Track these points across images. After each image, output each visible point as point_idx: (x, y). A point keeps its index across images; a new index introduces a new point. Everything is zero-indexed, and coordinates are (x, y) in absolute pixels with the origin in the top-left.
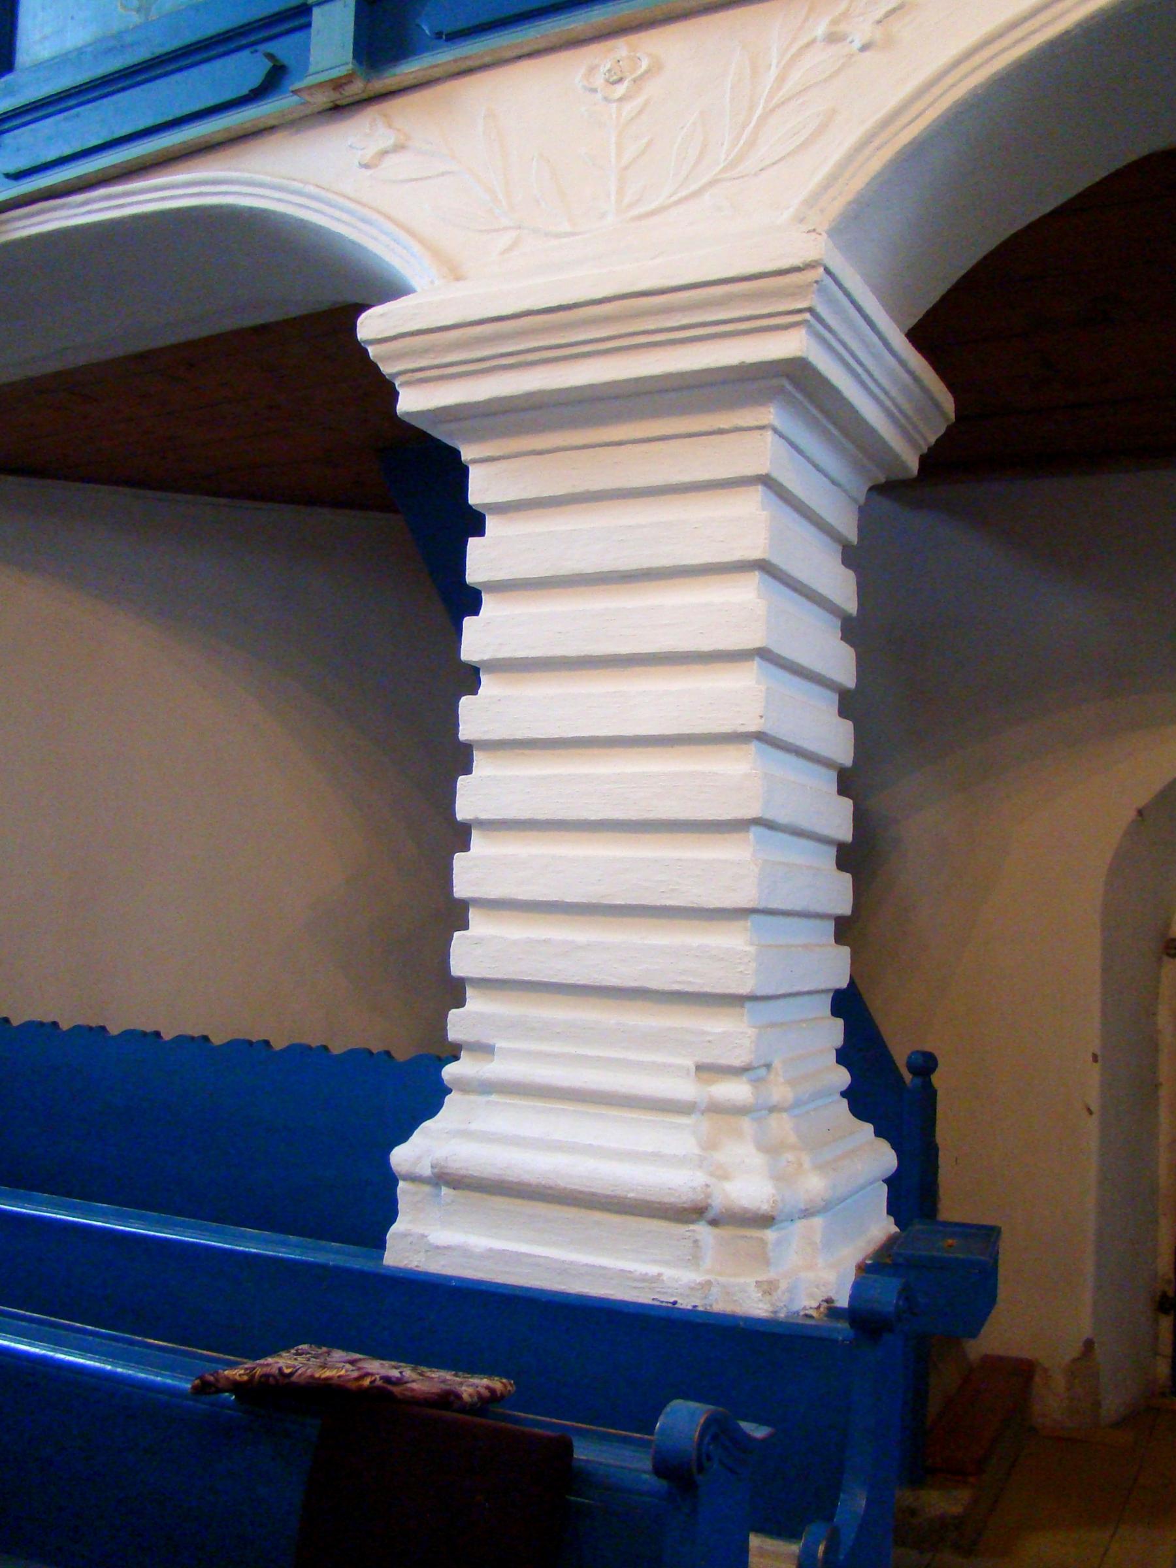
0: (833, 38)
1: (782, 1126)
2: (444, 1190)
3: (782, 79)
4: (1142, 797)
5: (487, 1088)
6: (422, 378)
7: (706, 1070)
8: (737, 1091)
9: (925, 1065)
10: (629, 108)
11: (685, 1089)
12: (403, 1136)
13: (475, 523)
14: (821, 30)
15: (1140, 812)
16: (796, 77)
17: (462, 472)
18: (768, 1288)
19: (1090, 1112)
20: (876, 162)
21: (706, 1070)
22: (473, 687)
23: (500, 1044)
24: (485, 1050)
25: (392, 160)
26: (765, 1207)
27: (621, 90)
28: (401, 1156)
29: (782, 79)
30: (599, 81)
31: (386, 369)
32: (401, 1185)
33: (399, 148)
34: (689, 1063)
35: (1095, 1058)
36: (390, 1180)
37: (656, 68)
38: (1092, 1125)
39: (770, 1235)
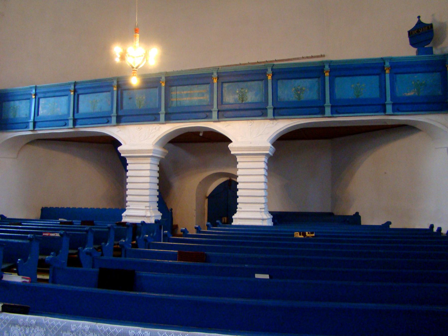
0: (155, 129)
1: (151, 211)
2: (127, 217)
3: (151, 131)
4: (200, 180)
5: (129, 209)
6: (123, 153)
7: (146, 207)
8: (148, 208)
9: (172, 210)
10: (140, 131)
11: (144, 208)
12: (123, 213)
13: (127, 164)
14: (154, 128)
15: (200, 182)
16: (152, 131)
17: (126, 160)
18: (150, 221)
19: (194, 216)
20: (159, 139)
21: (146, 207)
22: (128, 178)
23: (130, 205)
24: (129, 206)
25: (119, 132)
26: (150, 216)
27: (139, 130)
28: (123, 215)
29: (151, 131)
30: (137, 129)
31: (120, 152)
32: (123, 217)
33: (120, 131)
34: (144, 206)
35: (195, 210)
36: (122, 216)
37: (142, 128)
38: (195, 218)
39: (150, 218)
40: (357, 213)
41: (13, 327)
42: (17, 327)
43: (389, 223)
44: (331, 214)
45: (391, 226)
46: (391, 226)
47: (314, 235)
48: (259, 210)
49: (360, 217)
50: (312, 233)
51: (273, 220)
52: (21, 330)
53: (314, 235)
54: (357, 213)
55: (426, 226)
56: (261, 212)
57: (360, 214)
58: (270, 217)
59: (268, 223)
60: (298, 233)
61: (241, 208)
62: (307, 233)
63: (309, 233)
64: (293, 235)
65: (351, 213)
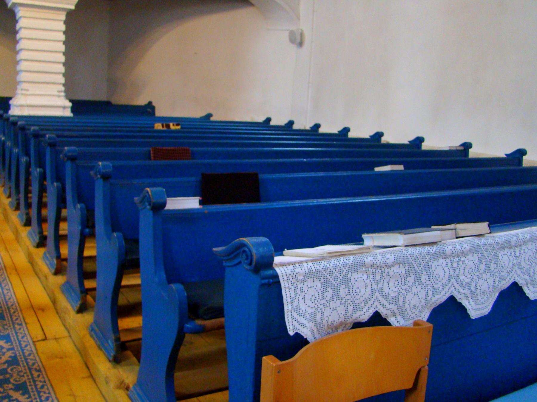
40: (150, 103)
41: (502, 253)
42: (507, 250)
43: (209, 115)
44: (108, 104)
45: (212, 119)
46: (212, 119)
47: (179, 127)
48: (58, 94)
49: (153, 108)
50: (177, 125)
51: (73, 110)
52: (511, 254)
53: (179, 127)
54: (150, 103)
55: (261, 119)
56: (59, 96)
57: (154, 104)
58: (70, 104)
59: (68, 113)
60: (160, 125)
61: (28, 90)
62: (171, 124)
63: (173, 125)
64: (153, 127)
65: (141, 101)
